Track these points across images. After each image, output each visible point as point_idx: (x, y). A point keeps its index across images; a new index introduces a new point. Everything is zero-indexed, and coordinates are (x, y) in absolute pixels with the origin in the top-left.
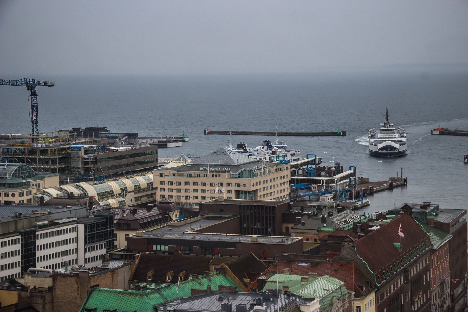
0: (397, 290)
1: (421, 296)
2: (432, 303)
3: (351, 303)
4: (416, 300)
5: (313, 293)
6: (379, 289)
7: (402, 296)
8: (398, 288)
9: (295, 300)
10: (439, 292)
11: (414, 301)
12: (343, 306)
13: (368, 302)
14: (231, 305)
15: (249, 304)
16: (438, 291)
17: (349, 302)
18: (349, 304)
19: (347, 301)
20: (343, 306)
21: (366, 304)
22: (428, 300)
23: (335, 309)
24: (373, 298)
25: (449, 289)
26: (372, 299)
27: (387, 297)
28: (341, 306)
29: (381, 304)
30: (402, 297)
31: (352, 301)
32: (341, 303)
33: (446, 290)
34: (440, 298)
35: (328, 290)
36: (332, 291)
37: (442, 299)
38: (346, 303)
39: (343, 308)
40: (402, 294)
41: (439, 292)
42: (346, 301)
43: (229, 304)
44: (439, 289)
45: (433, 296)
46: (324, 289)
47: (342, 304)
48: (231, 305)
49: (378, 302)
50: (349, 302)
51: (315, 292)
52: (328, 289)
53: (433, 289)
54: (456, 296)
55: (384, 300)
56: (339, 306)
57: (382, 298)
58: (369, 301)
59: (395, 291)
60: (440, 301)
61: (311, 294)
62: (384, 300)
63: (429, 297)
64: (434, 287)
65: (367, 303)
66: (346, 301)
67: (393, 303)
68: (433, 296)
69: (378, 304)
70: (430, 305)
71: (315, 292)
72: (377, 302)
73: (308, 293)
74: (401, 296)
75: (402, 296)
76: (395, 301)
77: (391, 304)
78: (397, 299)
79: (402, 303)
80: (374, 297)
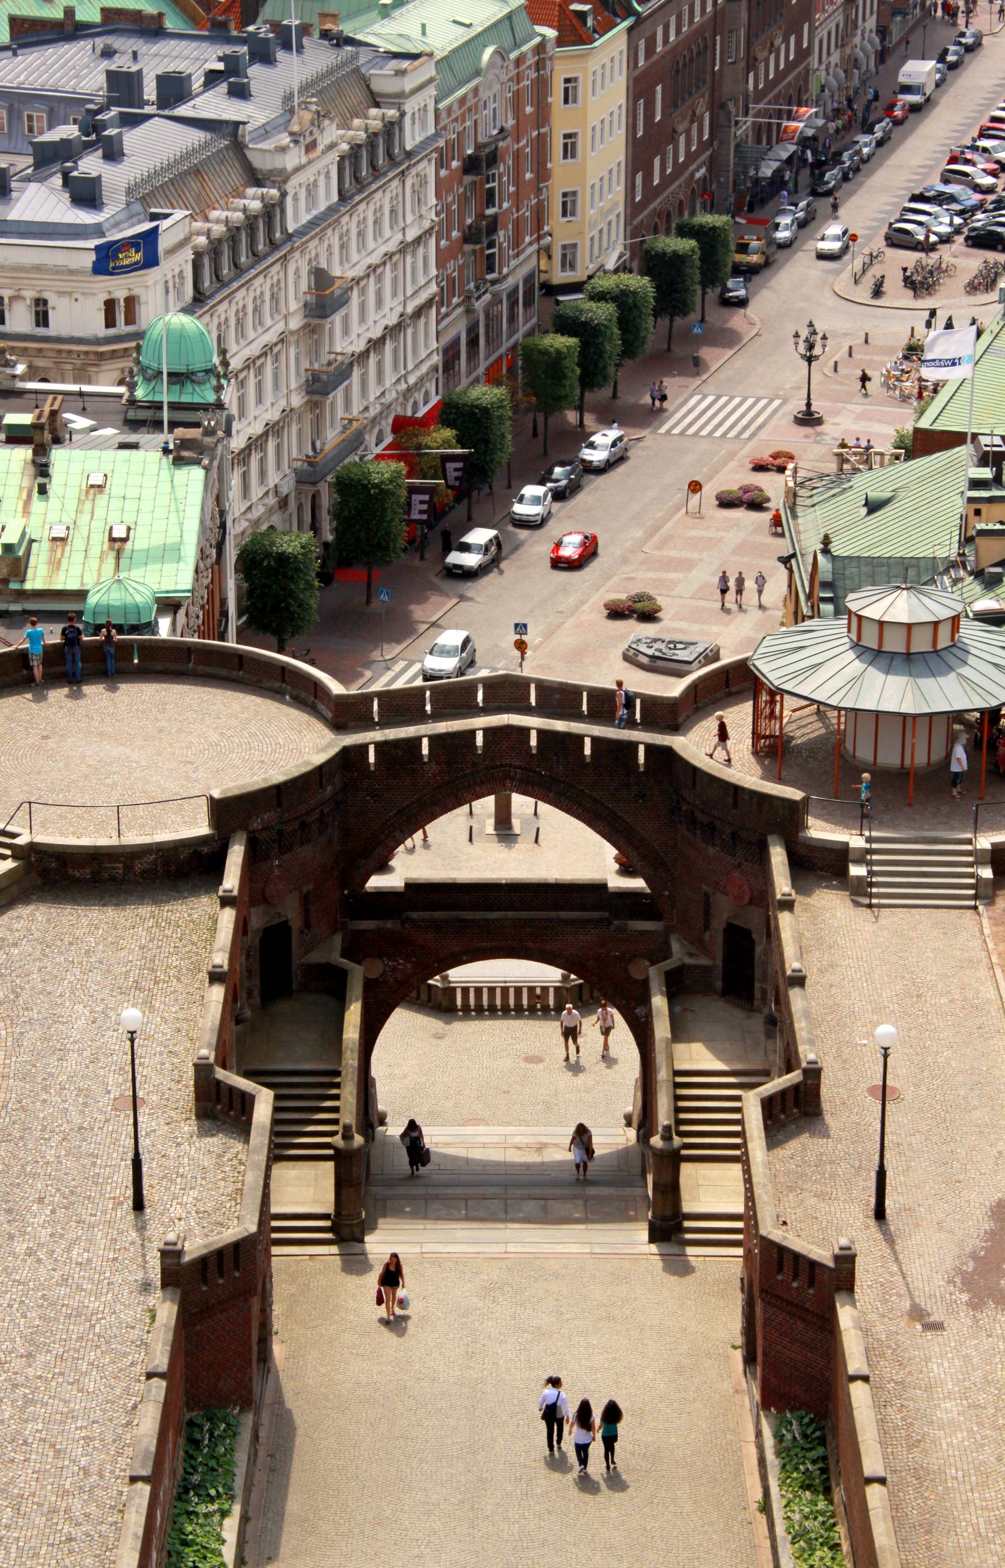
0: (702, 26)
1: (778, 41)
2: (816, 66)
3: (544, 68)
4: (761, 56)
5: (415, 33)
6: (640, 20)
7: (718, 42)
8: (706, 17)
9: (355, 57)
10: (841, 26)
11: (756, 60)
12: (518, 78)
13: (603, 66)
14: (140, 72)
15: (201, 72)
16: (837, 26)
17: (539, 66)
18: (538, 70)
19: (531, 60)
20: (518, 78)
21: (594, 73)
22: (803, 54)
23: (490, 87)
24: (621, 52)
25: (875, 17)
26: (615, 54)
27: (668, 47)
28: (511, 79)
29: (646, 73)
30: (718, 47)
31: (548, 63)
32: (511, 66)
33: (864, 20)
34: (842, 46)
35: (469, 26)
36: (480, 29)
37: (848, 50)
38: (529, 67)
39: (518, 83)
40: (718, 38)
41: (841, 26)
42: (528, 63)
43: (134, 69)
44: (840, 18)
45: (821, 42)
46: (455, 22)
47: (514, 72)
48: (140, 72)
49: (636, 63)
50: (539, 66)
51: (424, 33)
52: (468, 22)
53: (822, 18)
54: (894, 41)
55: (655, 58)
56: (504, 78)
57: (650, 50)
58: (607, 61)
59: (694, 27)
60: (842, 58)
61: (408, 38)
62: (655, 58)
63: (805, 45)
64: (824, 11)
65: (598, 67)
66: (528, 63)
67: (685, 65)
68: (821, 42)
69: (637, 72)
70: (807, 70)
71: (424, 33)
72: (632, 64)
73: (401, 35)
74: (715, 45)
75: (718, 42)
76: (691, 60)
77: (678, 71)
78: (699, 54)
79: (717, 68)
80: (624, 47)
